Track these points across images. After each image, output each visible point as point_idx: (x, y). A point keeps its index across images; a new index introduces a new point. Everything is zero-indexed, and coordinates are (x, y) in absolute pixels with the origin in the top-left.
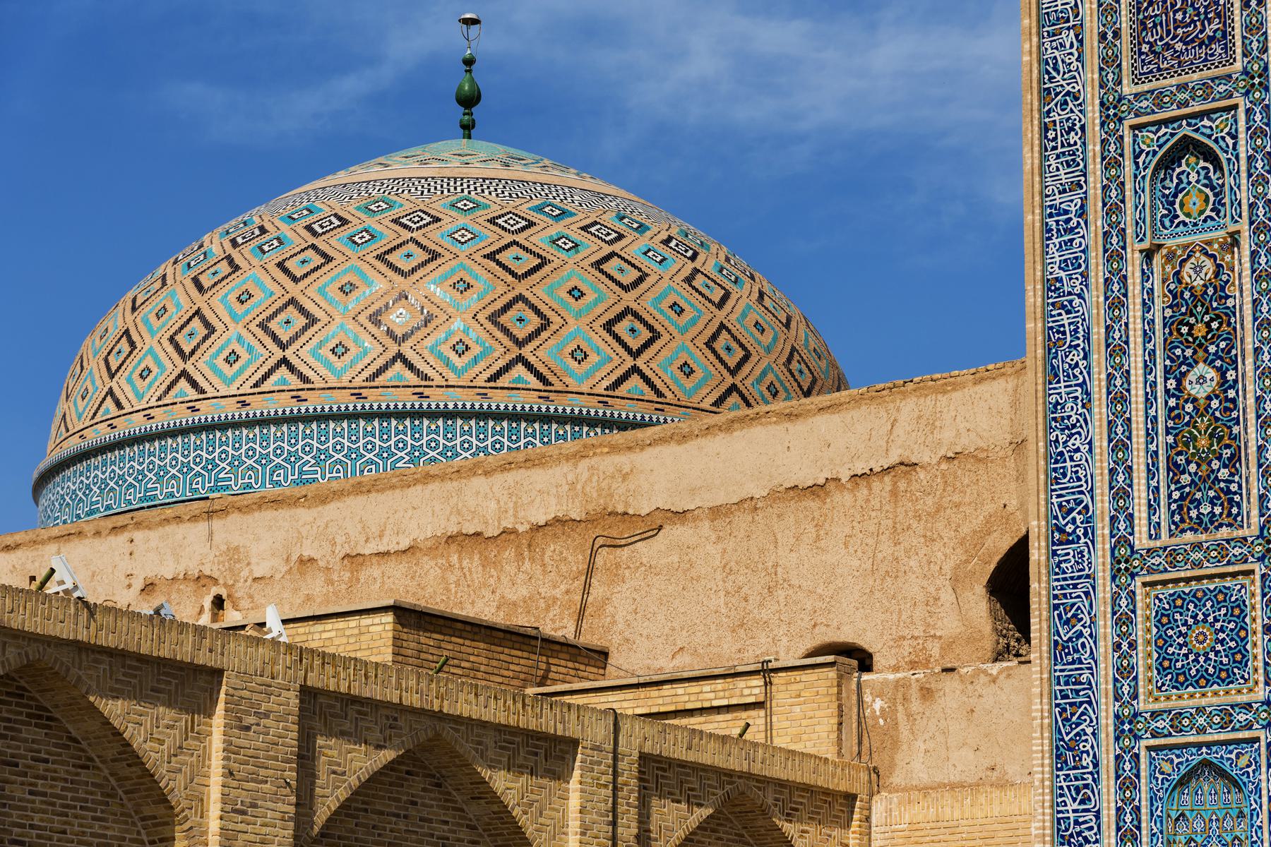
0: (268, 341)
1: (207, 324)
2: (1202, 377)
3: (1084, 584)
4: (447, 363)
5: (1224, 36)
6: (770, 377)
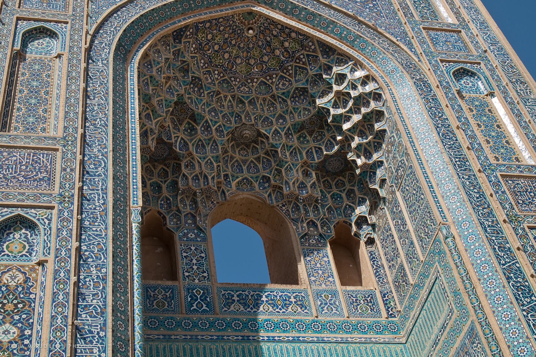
2: (7, 330)
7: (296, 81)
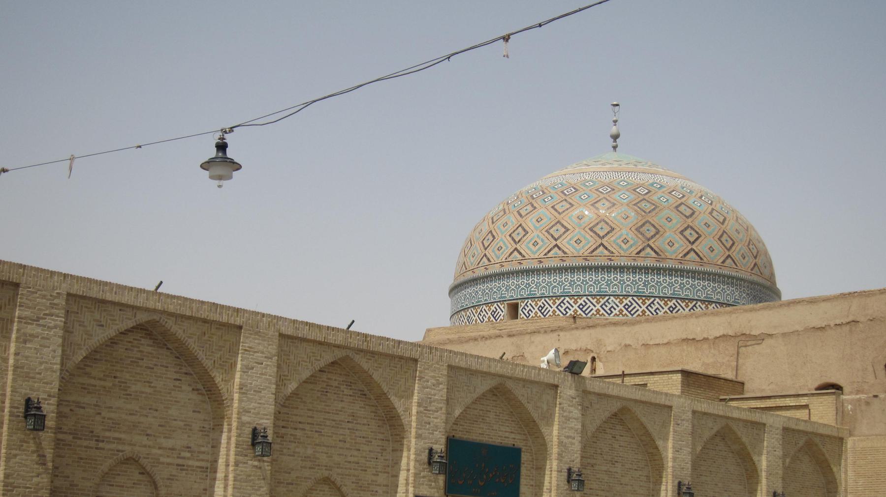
0: (550, 237)
1: (524, 230)
4: (620, 247)
6: (742, 251)
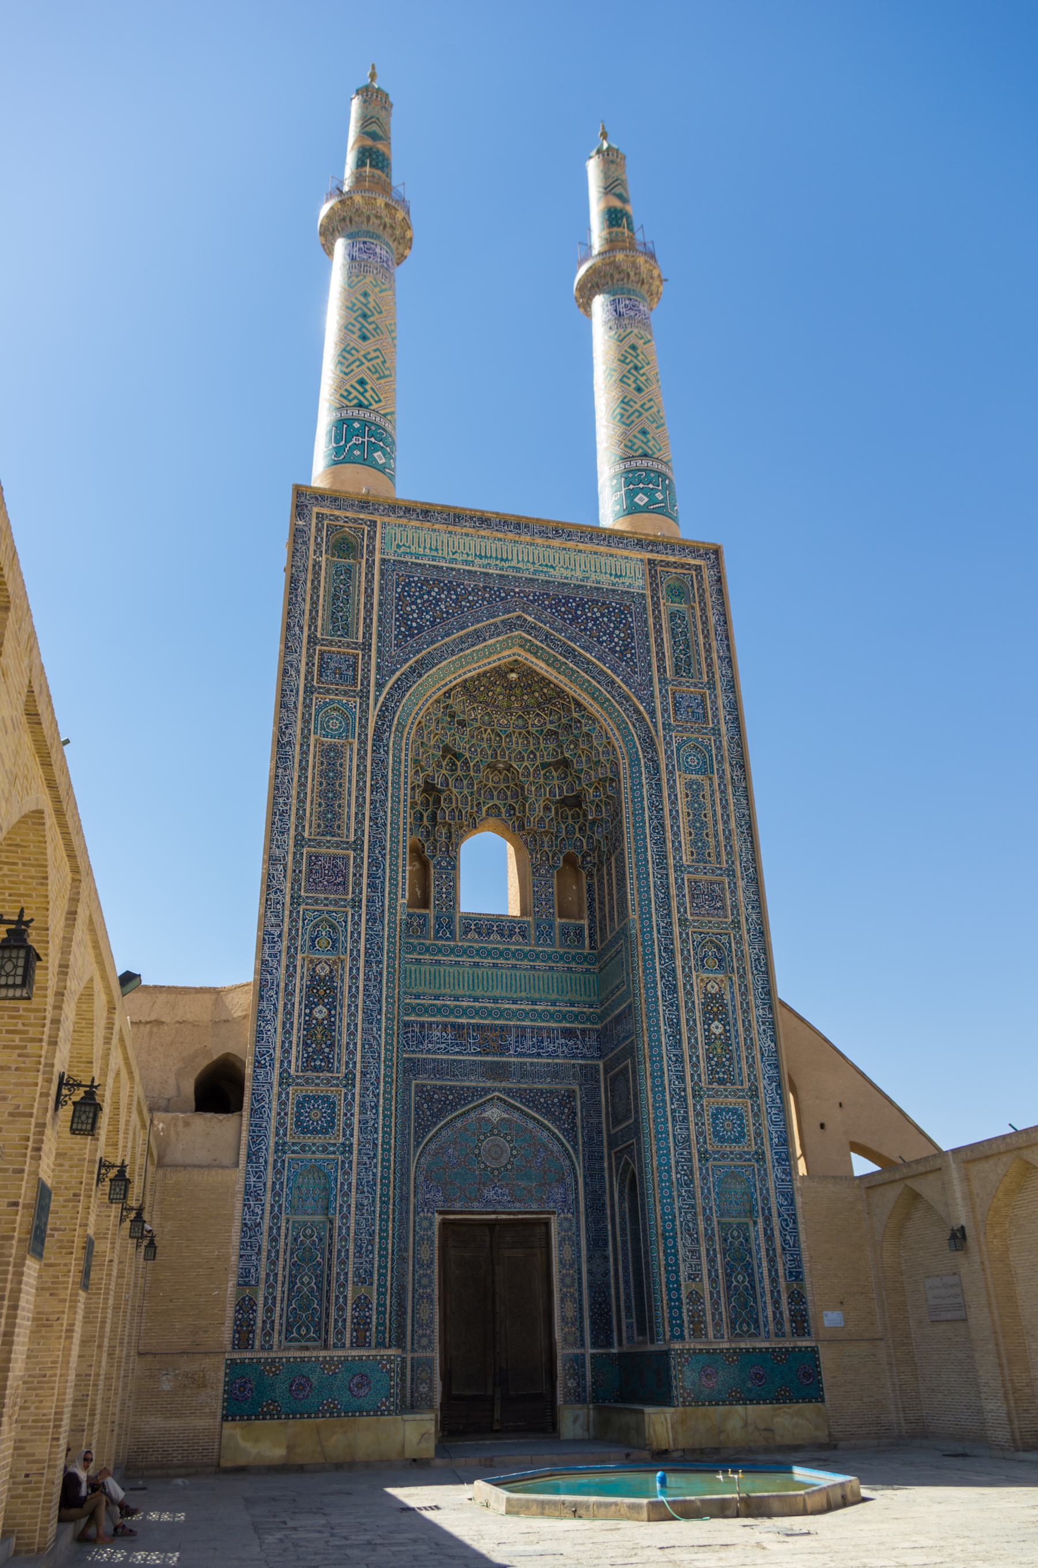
3: (267, 1086)
5: (344, 884)
7: (551, 722)
